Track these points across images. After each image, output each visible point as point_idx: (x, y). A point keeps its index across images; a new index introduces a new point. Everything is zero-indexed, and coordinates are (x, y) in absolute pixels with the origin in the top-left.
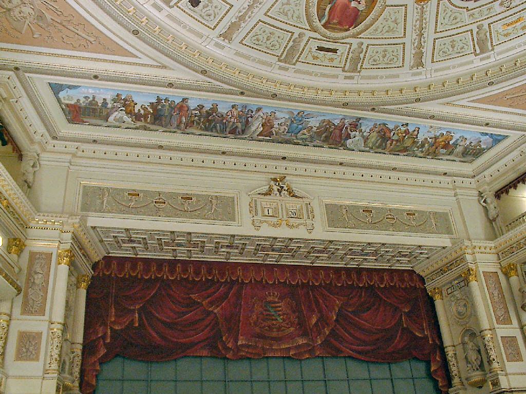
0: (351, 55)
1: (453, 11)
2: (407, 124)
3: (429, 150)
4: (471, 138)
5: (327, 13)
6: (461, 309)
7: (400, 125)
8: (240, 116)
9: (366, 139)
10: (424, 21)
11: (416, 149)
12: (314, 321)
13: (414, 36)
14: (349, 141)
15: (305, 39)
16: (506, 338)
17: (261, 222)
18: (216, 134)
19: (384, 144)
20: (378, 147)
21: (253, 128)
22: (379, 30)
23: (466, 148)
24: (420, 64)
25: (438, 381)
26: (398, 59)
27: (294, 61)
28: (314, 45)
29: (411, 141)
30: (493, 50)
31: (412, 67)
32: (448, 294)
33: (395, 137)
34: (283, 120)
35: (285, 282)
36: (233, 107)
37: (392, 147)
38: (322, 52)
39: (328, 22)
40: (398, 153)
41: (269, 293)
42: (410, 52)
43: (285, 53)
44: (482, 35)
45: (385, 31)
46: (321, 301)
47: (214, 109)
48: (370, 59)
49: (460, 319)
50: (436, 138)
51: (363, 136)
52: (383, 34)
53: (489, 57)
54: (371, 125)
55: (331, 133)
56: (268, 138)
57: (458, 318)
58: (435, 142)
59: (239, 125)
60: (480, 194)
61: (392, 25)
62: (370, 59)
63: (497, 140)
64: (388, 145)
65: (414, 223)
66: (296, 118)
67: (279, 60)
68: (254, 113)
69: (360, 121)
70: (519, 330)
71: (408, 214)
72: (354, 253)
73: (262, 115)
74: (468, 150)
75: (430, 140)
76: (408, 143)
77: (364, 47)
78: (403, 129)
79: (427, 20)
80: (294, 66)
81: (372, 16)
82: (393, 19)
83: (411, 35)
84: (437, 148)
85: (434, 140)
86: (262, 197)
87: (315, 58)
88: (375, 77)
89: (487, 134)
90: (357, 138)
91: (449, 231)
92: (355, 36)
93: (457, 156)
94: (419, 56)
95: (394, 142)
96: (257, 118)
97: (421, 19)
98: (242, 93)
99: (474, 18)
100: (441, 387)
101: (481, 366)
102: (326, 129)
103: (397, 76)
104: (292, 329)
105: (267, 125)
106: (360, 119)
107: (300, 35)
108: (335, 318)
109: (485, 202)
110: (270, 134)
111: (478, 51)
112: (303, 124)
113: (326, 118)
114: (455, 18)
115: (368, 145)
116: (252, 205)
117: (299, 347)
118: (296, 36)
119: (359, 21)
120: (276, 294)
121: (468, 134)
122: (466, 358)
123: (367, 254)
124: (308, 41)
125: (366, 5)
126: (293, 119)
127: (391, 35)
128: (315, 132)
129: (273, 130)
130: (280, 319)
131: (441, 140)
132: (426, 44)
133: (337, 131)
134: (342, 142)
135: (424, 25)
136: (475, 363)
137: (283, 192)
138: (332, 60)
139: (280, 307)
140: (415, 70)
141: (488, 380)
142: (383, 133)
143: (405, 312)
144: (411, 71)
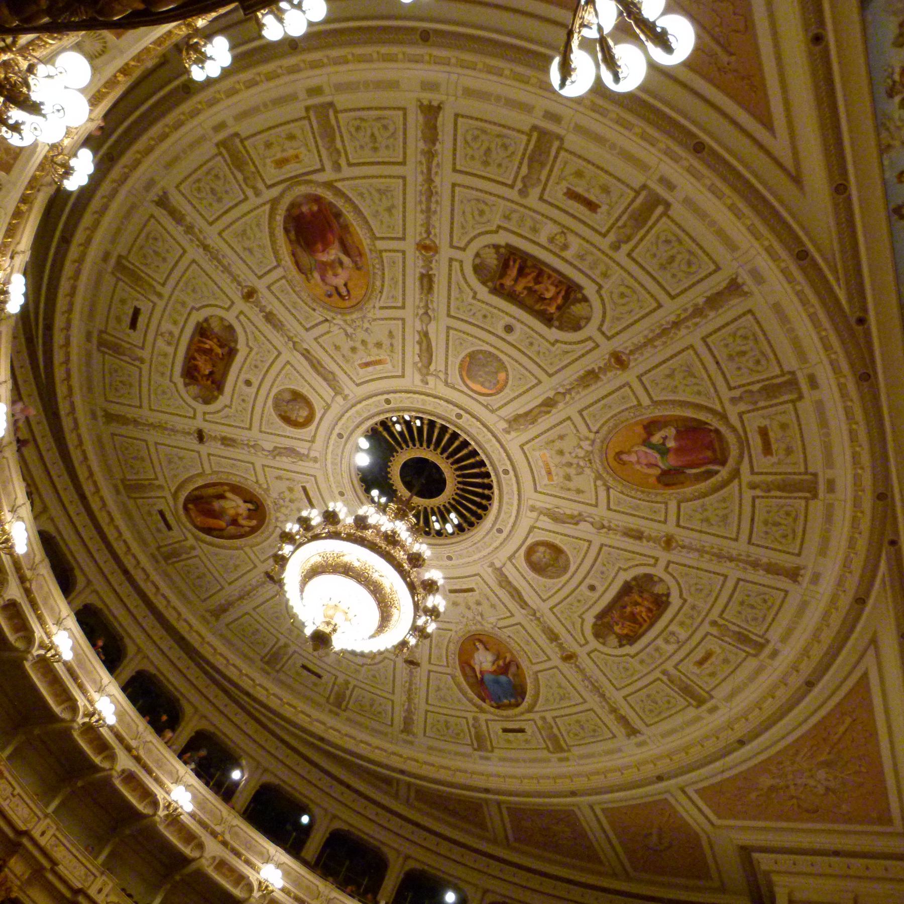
5: (702, 469)
10: (651, 336)
13: (683, 331)
15: (757, 479)
22: (696, 388)
24: (734, 287)
27: (808, 477)
28: (763, 463)
30: (644, 187)
31: (746, 294)
38: (774, 446)
39: (714, 461)
42: (715, 319)
43: (795, 495)
44: (628, 231)
45: (694, 380)
48: (759, 372)
52: (702, 379)
61: (679, 376)
62: (759, 372)
67: (815, 496)
77: (737, 393)
79: (646, 332)
80: (820, 474)
81: (678, 412)
87: (789, 451)
92: (724, 417)
94: (714, 301)
98: (893, 543)
99: (608, 267)
103: (777, 308)
107: (753, 486)
111: (660, 209)
114: (622, 295)
118: (758, 492)
119: (694, 424)
124: (761, 473)
125: (666, 426)
135: (657, 331)
138: (784, 427)
140: (749, 284)
144: (754, 289)
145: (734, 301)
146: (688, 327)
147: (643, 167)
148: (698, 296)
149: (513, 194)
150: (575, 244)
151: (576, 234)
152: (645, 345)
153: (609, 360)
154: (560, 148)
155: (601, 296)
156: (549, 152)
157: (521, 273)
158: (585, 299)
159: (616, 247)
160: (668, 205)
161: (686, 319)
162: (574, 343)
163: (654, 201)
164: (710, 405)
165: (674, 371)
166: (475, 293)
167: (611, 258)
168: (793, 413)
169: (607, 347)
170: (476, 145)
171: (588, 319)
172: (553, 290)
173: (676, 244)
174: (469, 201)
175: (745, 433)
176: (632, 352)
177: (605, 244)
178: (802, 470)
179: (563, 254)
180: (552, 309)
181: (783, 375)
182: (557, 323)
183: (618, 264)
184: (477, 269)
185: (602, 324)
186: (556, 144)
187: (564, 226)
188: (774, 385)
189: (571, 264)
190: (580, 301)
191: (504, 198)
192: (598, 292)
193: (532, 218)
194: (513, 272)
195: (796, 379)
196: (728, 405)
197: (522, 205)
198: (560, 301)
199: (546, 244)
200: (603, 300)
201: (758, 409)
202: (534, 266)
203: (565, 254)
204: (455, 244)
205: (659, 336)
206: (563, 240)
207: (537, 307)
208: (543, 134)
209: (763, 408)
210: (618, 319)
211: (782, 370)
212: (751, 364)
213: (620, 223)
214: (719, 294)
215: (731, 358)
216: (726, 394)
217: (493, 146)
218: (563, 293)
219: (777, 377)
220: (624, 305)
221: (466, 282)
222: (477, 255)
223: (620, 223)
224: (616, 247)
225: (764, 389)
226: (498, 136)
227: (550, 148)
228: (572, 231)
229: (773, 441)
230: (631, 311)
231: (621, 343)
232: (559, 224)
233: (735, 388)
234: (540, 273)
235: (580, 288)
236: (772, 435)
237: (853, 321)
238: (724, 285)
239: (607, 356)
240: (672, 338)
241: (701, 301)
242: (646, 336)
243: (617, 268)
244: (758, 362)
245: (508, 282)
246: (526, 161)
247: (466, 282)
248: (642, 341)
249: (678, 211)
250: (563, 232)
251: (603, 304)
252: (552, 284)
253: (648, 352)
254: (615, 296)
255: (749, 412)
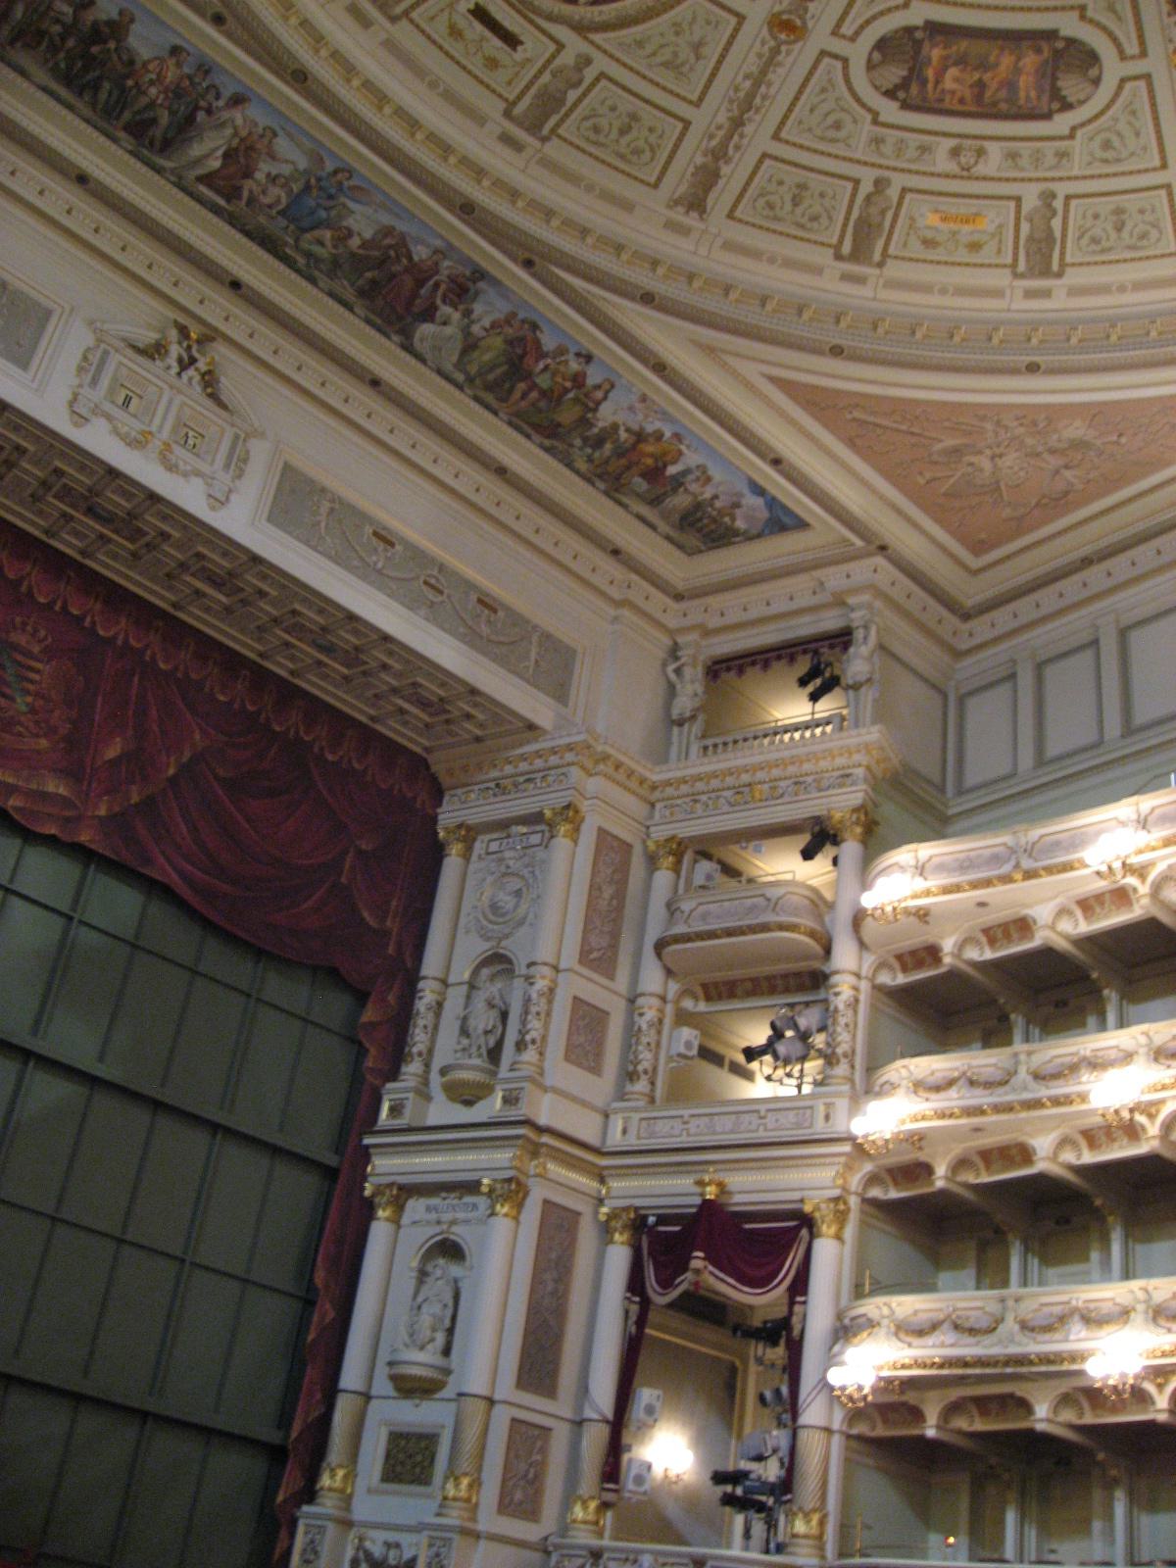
0: (546, 77)
1: (842, 103)
2: (588, 358)
3: (607, 462)
4: (720, 484)
6: (506, 900)
7: (573, 349)
8: (177, 92)
9: (470, 346)
10: (763, 89)
11: (578, 442)
12: (112, 752)
13: (722, 118)
14: (426, 329)
16: (586, 1008)
17: (97, 410)
18: (87, 112)
19: (507, 385)
20: (489, 387)
21: (196, 150)
23: (698, 506)
24: (696, 203)
25: (367, 1050)
26: (652, 159)
27: (398, 10)
29: (577, 410)
30: (880, 265)
31: (677, 202)
32: (488, 854)
33: (543, 381)
34: (286, 170)
35: (80, 619)
36: (175, 51)
37: (523, 404)
40: (530, 431)
41: (25, 624)
42: (691, 155)
44: (873, 210)
45: (659, 59)
46: (154, 712)
47: (117, 29)
48: (586, 118)
49: (491, 922)
50: (640, 437)
51: (466, 332)
52: (650, 66)
53: (860, 280)
54: (500, 308)
55: (393, 276)
56: (222, 202)
57: (485, 917)
58: (634, 446)
59: (164, 118)
60: (674, 652)
61: (686, 53)
62: (586, 118)
63: (781, 521)
64: (517, 394)
65: (485, 630)
66: (323, 184)
68: (221, 103)
69: (482, 285)
70: (622, 1004)
71: (480, 601)
72: (297, 629)
73: (239, 121)
74: (699, 514)
75: (623, 435)
76: (567, 415)
77: (589, 74)
78: (574, 366)
79: (772, 91)
80: (388, 25)
82: (696, 38)
83: (711, 115)
84: (628, 468)
85: (633, 439)
86: (130, 352)
87: (455, 32)
88: (573, 178)
89: (759, 490)
90: (449, 330)
91: (560, 693)
92: (581, 28)
93: (665, 516)
94: (707, 178)
95: (534, 395)
96: (223, 125)
97: (759, 79)
98: (218, 20)
100: (372, 1070)
101: (494, 1054)
102: (381, 263)
103: (628, 206)
104: (44, 743)
105: (241, 157)
106: (479, 274)
108: (171, 771)
109: (678, 671)
110: (233, 194)
111: (846, 248)
112: (333, 213)
113: (402, 226)
114: (837, 126)
115: (468, 368)
116: (90, 357)
117: (44, 796)
120: (42, 633)
121: (718, 467)
122: (465, 1019)
123: (329, 649)
126: (313, 181)
127: (666, 78)
128: (353, 255)
129: (248, 185)
130: (22, 703)
131: (649, 448)
132: (737, 155)
133: (408, 281)
134: (409, 319)
135: (758, 101)
136: (482, 1040)
137: (191, 372)
138: (492, 63)
139: (38, 671)
140: (678, 215)
141: (498, 1087)
142: (519, 351)
143: (360, 852)
145: (682, 189)
146: (719, 128)
147: (891, 284)
148: (733, 175)
149: (1062, 189)
150: (943, 162)
151: (947, 176)
152: (764, 72)
153: (804, 23)
154: (1014, 264)
155: (870, 110)
156: (1028, 254)
157: (1011, 85)
158: (890, 94)
159: (880, 184)
160: (838, 257)
161: (729, 137)
162: (874, 18)
163: (859, 254)
164: (611, 35)
165: (698, 57)
166: (1083, 17)
167: (880, 166)
168: (499, 89)
169: (819, 37)
170: (1142, 227)
171: (871, 66)
172: (948, 83)
173: (803, 221)
174: (1132, 154)
175: (531, 22)
176: (775, 51)
177: (898, 181)
178: (414, 15)
179: (952, 143)
180: (936, 54)
181: (553, 131)
182: (919, 35)
183: (866, 163)
184: (1092, 58)
185: (846, 68)
186: (1022, 267)
187: (969, 178)
188: (554, 111)
189: (936, 133)
190: (897, 87)
191: (1076, 178)
192: (875, 114)
193: (1022, 169)
194: (1025, 83)
195: (534, 135)
196: (584, 47)
197: (1046, 179)
198: (930, 73)
199: (986, 144)
200: (863, 105)
201: (545, 67)
202: (995, 104)
203: (952, 143)
204: (1142, 84)
205: (751, 95)
206: (963, 160)
207: (964, 45)
208: (1046, 272)
209: (540, 72)
210: (823, 90)
211: (559, 137)
212: (603, 122)
213: (889, 215)
214: (708, 189)
215: (634, 117)
216: (601, 63)
217: (1113, 235)
218: (930, 86)
219: (558, 125)
220: (827, 114)
221: (1104, 29)
222: (1096, 82)
223: (889, 215)
224: (880, 184)
225: (562, 101)
226: (1110, 249)
227: (1028, 261)
228: (955, 177)
229: (488, 34)
230: (812, 110)
231: (799, 58)
232: (977, 178)
233: (597, 80)
234: (979, 98)
235: (906, 106)
236: (497, 43)
237: (536, 259)
238: (710, 201)
239: (810, 24)
240: (731, 101)
241: (725, 170)
242: (769, 85)
243: (862, 158)
244: (596, 129)
245: (1030, 61)
246: (1058, 234)
247: (1104, 29)
248: (771, 76)
249: (824, 257)
250: (968, 170)
251: (858, 100)
252: (953, 93)
253: (752, 65)
254: (847, 119)
255: (553, 57)
